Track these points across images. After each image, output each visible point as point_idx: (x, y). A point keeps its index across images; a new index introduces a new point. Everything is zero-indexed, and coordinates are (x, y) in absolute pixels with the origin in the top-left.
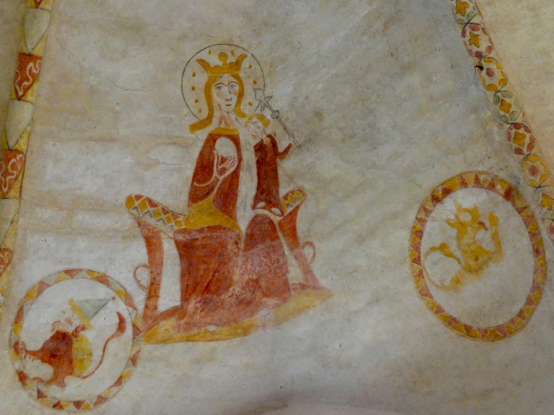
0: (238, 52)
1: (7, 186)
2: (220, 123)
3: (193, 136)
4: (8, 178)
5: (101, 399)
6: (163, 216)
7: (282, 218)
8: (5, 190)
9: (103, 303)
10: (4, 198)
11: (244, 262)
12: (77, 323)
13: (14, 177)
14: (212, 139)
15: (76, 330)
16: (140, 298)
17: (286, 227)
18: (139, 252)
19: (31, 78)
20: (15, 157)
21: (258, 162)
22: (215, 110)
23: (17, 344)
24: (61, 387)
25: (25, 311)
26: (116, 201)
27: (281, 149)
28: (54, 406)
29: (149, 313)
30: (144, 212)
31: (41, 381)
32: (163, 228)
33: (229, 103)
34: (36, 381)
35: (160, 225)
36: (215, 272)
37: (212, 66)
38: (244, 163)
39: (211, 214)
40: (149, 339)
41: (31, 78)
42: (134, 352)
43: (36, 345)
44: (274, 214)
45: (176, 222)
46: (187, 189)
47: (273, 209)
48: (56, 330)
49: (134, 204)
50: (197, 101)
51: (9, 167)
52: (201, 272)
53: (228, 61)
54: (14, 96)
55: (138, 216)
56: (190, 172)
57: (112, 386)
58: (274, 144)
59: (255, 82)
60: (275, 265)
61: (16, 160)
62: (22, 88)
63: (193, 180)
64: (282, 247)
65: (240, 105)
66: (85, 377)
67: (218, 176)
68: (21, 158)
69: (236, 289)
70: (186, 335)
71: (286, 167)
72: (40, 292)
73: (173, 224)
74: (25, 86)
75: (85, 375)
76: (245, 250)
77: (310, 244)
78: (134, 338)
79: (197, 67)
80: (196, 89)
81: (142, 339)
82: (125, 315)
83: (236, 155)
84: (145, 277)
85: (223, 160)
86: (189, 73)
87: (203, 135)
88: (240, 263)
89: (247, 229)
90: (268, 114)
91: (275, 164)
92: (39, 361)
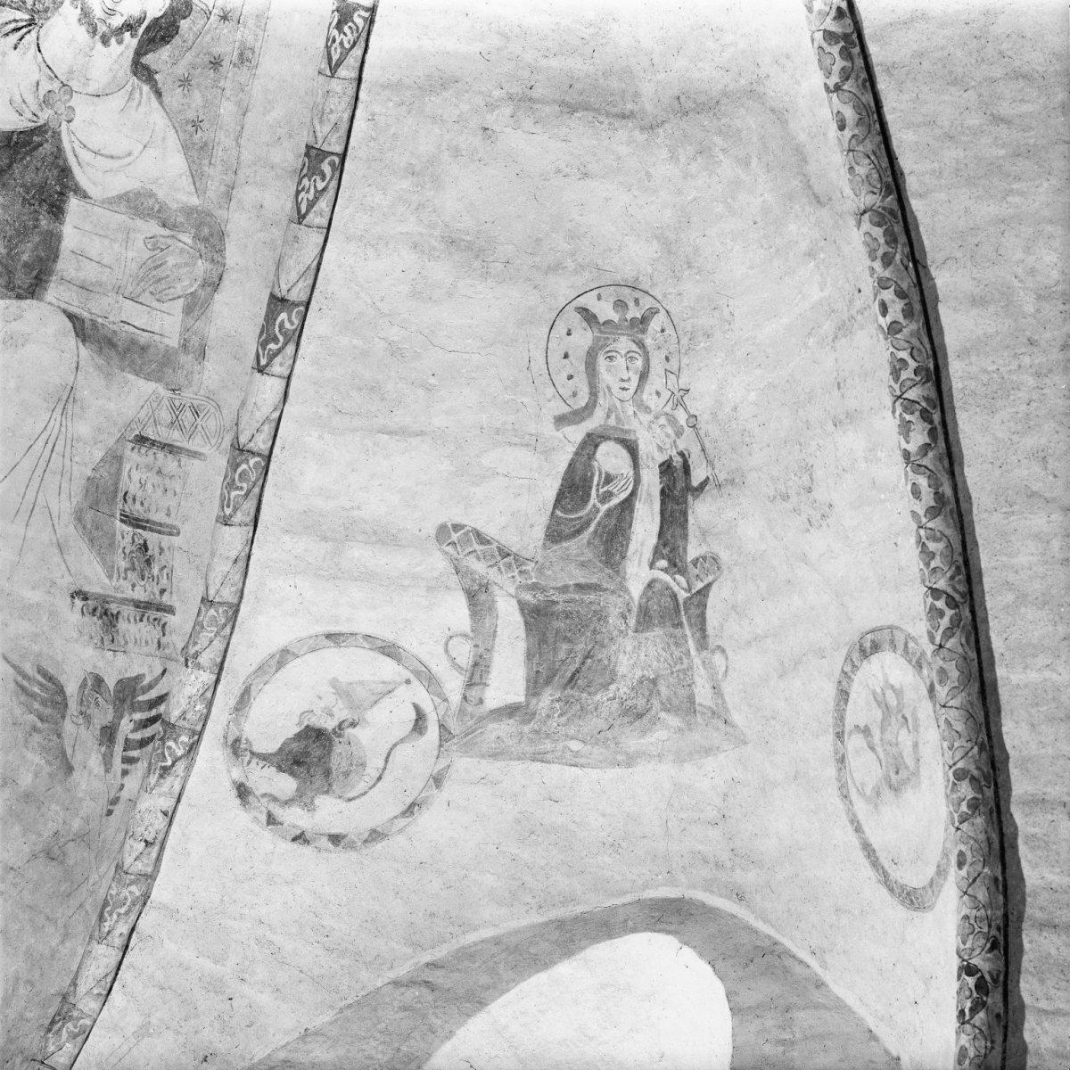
0: (647, 302)
2: (608, 417)
3: (559, 434)
4: (234, 494)
5: (375, 835)
7: (689, 595)
9: (390, 687)
10: (226, 525)
11: (634, 647)
12: (342, 713)
13: (243, 493)
14: (591, 442)
15: (340, 726)
16: (454, 685)
17: (694, 611)
18: (456, 612)
19: (281, 338)
21: (662, 492)
22: (601, 395)
23: (237, 740)
24: (309, 810)
25: (253, 693)
26: (420, 531)
27: (695, 483)
28: (294, 840)
29: (470, 709)
30: (467, 551)
31: (275, 799)
33: (625, 385)
34: (266, 799)
35: (493, 575)
36: (587, 657)
37: (601, 320)
38: (642, 490)
39: (583, 565)
40: (468, 748)
41: (281, 338)
42: (440, 766)
44: (678, 584)
45: (520, 572)
46: (542, 521)
47: (678, 577)
48: (305, 724)
49: (450, 537)
50: (570, 377)
52: (562, 655)
53: (629, 316)
55: (456, 555)
56: (551, 495)
57: (396, 817)
58: (686, 469)
59: (667, 359)
60: (678, 667)
62: (266, 353)
63: (554, 508)
64: (687, 642)
65: (642, 392)
66: (350, 800)
67: (599, 505)
69: (622, 688)
70: (530, 750)
71: (701, 511)
72: (281, 664)
73: (516, 573)
74: (270, 350)
75: (350, 795)
76: (636, 631)
77: (723, 651)
78: (441, 746)
79: (576, 318)
80: (571, 358)
81: (455, 748)
82: (427, 707)
83: (632, 472)
84: (464, 653)
85: (609, 479)
86: (561, 328)
87: (576, 433)
88: (629, 649)
89: (641, 598)
90: (681, 416)
91: (686, 502)
92: (273, 769)
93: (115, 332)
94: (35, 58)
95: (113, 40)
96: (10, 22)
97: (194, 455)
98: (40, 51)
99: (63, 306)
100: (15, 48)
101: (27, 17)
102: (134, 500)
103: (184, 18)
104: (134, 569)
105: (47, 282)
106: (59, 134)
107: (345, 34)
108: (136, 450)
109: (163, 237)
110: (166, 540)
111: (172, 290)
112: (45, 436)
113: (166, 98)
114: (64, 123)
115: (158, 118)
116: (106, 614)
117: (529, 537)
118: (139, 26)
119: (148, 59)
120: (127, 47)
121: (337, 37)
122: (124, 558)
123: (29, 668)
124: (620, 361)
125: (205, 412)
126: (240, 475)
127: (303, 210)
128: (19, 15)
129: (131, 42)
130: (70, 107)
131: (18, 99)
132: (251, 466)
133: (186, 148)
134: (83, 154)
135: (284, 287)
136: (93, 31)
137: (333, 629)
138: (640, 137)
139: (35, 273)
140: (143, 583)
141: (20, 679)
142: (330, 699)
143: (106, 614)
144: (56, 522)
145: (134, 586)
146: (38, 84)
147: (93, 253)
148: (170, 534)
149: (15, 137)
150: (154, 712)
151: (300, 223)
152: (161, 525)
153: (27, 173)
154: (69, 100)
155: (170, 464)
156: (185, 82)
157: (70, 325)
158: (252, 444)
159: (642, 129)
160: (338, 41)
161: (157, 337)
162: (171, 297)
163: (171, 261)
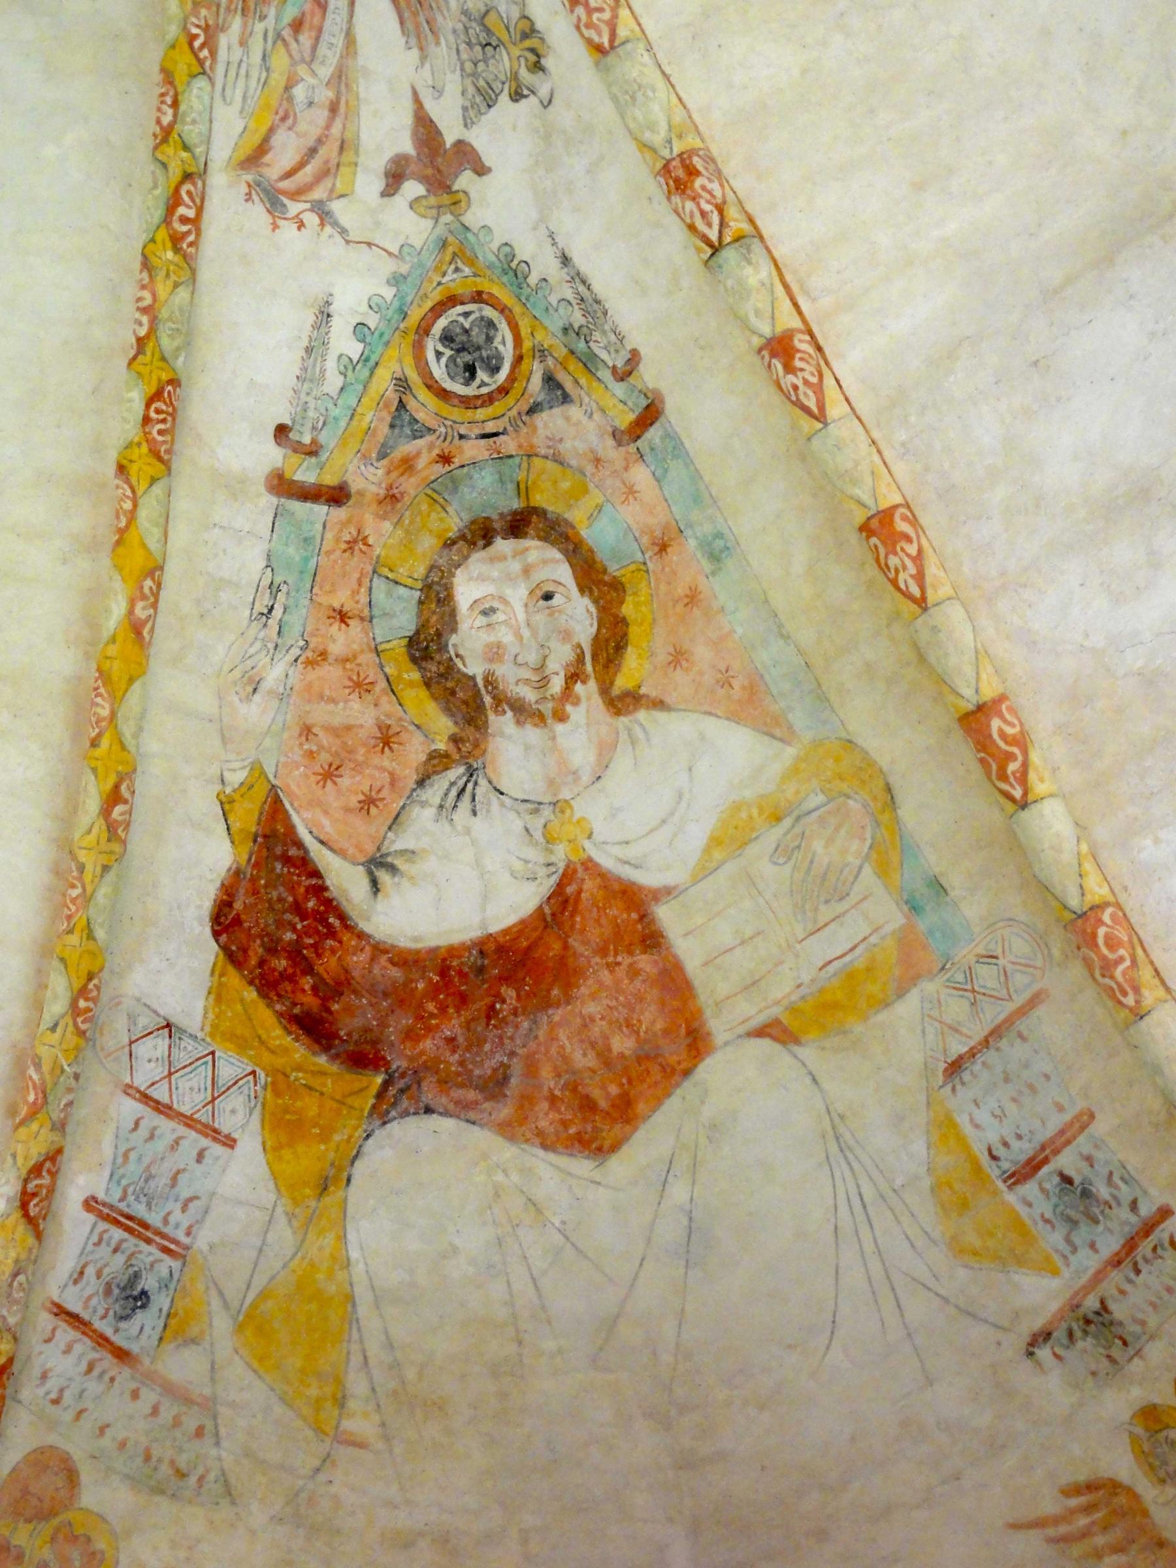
1: (1129, 990)
4: (1118, 972)
8: (1130, 1000)
10: (1141, 1018)
13: (1128, 963)
19: (1015, 750)
20: (1100, 922)
41: (1015, 750)
51: (1105, 951)
54: (1010, 807)
61: (1108, 926)
62: (1012, 780)
68: (1113, 916)
74: (1013, 773)
93: (821, 991)
94: (503, 805)
95: (569, 708)
96: (448, 790)
98: (502, 793)
99: (741, 1030)
100: (475, 813)
101: (461, 769)
102: (1006, 1144)
103: (622, 603)
104: (1074, 1223)
105: (703, 1024)
106: (590, 859)
107: (802, 370)
108: (959, 1087)
109: (788, 832)
110: (1082, 1143)
111: (846, 872)
112: (841, 1196)
114: (587, 844)
116: (1088, 1322)
118: (584, 664)
119: (622, 682)
120: (589, 699)
121: (795, 381)
122: (1053, 1227)
123: (1050, 1505)
125: (1000, 944)
126: (1107, 944)
127: (915, 591)
129: (588, 690)
130: (578, 822)
131: (518, 865)
132: (1109, 922)
133: (734, 717)
134: (631, 853)
135: (968, 692)
136: (539, 718)
139: (683, 1031)
140: (1101, 1228)
141: (1051, 1532)
143: (1088, 1322)
144: (932, 1283)
145: (1092, 1246)
146: (527, 830)
147: (728, 939)
148: (1083, 1128)
149: (547, 910)
151: (925, 609)
152: (1062, 1132)
154: (572, 815)
155: (1012, 1051)
157: (766, 1043)
158: (1088, 897)
160: (800, 383)
161: (873, 939)
162: (851, 879)
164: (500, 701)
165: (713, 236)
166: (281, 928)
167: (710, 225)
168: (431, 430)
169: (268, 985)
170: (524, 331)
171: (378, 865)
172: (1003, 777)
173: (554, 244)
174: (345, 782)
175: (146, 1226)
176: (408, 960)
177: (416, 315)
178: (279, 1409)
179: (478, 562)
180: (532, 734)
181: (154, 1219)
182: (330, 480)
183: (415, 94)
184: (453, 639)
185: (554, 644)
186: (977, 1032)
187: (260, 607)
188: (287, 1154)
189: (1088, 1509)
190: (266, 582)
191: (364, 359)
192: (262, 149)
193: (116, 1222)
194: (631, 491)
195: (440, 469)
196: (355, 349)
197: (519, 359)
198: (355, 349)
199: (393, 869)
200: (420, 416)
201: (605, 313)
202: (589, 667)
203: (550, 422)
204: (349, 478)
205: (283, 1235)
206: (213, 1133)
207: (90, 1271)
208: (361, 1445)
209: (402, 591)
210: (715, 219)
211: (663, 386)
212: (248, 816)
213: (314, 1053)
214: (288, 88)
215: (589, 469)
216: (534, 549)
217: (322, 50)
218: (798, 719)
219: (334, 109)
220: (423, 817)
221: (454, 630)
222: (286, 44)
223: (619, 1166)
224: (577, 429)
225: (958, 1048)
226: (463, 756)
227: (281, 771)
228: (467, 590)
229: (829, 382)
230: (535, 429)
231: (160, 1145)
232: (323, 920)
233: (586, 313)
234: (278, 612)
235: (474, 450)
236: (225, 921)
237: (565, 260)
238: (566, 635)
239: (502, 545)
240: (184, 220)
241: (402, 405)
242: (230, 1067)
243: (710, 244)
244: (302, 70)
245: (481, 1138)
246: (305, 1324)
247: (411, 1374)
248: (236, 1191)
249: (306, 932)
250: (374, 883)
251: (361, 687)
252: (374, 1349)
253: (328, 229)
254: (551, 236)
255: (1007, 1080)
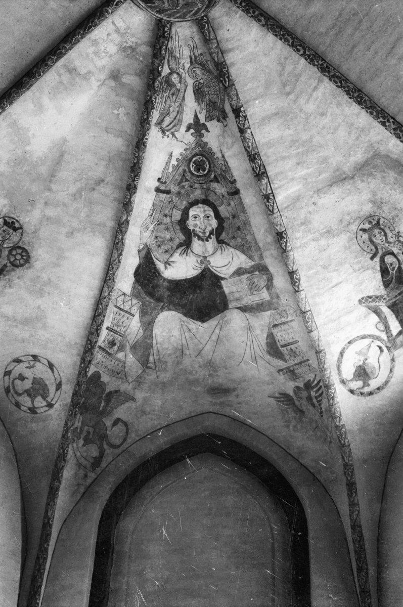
0: (376, 218)
4: (309, 324)
5: (387, 382)
6: (377, 300)
12: (362, 359)
16: (384, 336)
18: (374, 318)
31: (360, 388)
32: (380, 304)
43: (351, 376)
46: (381, 284)
53: (373, 224)
56: (380, 277)
59: (389, 228)
75: (376, 376)
79: (361, 233)
80: (366, 242)
85: (391, 264)
86: (359, 237)
87: (377, 259)
92: (355, 382)
93: (252, 305)
95: (209, 239)
97: (291, 321)
104: (292, 356)
110: (296, 345)
112: (249, 339)
113: (231, 244)
114: (209, 266)
115: (232, 250)
117: (382, 291)
119: (221, 238)
123: (277, 395)
124: (378, 235)
127: (285, 248)
128: (183, 247)
131: (195, 267)
136: (202, 240)
137: (349, 340)
138: (351, 181)
142: (358, 357)
145: (294, 360)
150: (319, 386)
153: (206, 283)
155: (286, 327)
156: (233, 238)
159: (350, 179)
163: (256, 280)
164: (196, 235)
165: (257, 172)
166: (147, 274)
167: (257, 169)
168: (189, 181)
169: (143, 286)
170: (212, 166)
171: (167, 263)
172: (294, 285)
173: (221, 152)
174: (162, 247)
175: (116, 331)
176: (170, 281)
177: (189, 157)
178: (137, 362)
179: (194, 208)
180: (201, 242)
181: (118, 330)
182: (167, 189)
183: (195, 111)
184: (187, 222)
185: (208, 226)
186: (279, 321)
187: (150, 214)
188: (144, 317)
189: (285, 397)
190: (152, 209)
191: (177, 165)
192: (162, 121)
193: (112, 331)
194: (229, 204)
195: (190, 188)
196: (176, 163)
197: (209, 171)
198: (176, 163)
199: (170, 265)
200: (187, 178)
201: (230, 170)
202: (214, 233)
203: (214, 185)
204: (171, 189)
205: (141, 331)
206: (130, 314)
207: (106, 340)
208: (151, 368)
209: (178, 211)
210: (258, 168)
211: (240, 189)
212: (144, 252)
213: (151, 299)
214: (169, 108)
215: (221, 197)
216: (207, 208)
217: (178, 100)
218: (256, 258)
219: (178, 112)
220: (176, 255)
221: (188, 220)
222: (170, 98)
223: (206, 325)
224: (220, 189)
225: (276, 323)
226: (186, 245)
227: (151, 246)
228: (192, 213)
229: (275, 205)
230: (210, 185)
231: (121, 317)
232: (154, 273)
233: (226, 168)
234: (153, 215)
235: (197, 185)
236: (137, 274)
237: (223, 156)
238: (211, 225)
239: (200, 205)
240: (146, 139)
241: (184, 175)
242: (135, 301)
243: (256, 173)
244: (173, 104)
245: (180, 315)
246: (143, 348)
247: (161, 357)
248: (134, 326)
249: (151, 276)
250: (166, 268)
251: (168, 229)
252: (155, 352)
253: (174, 138)
254: (221, 150)
255: (284, 331)
